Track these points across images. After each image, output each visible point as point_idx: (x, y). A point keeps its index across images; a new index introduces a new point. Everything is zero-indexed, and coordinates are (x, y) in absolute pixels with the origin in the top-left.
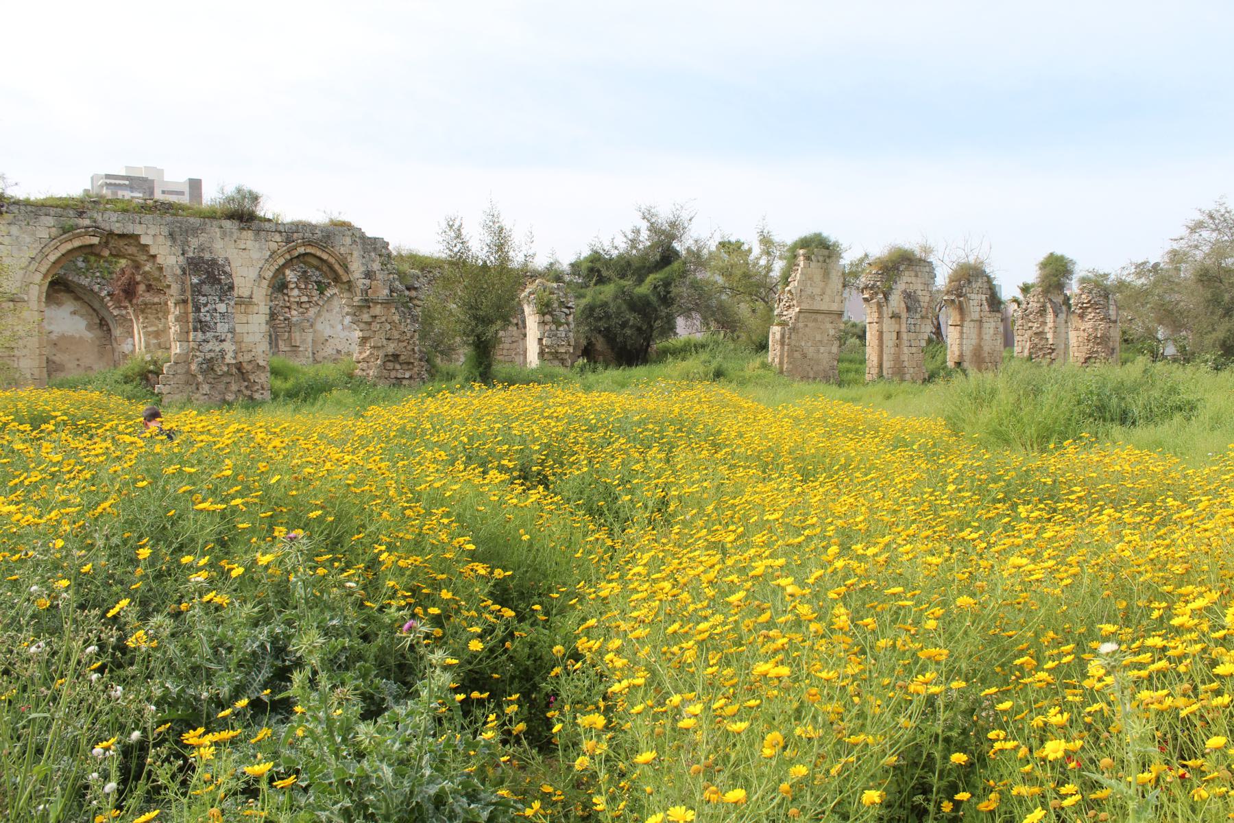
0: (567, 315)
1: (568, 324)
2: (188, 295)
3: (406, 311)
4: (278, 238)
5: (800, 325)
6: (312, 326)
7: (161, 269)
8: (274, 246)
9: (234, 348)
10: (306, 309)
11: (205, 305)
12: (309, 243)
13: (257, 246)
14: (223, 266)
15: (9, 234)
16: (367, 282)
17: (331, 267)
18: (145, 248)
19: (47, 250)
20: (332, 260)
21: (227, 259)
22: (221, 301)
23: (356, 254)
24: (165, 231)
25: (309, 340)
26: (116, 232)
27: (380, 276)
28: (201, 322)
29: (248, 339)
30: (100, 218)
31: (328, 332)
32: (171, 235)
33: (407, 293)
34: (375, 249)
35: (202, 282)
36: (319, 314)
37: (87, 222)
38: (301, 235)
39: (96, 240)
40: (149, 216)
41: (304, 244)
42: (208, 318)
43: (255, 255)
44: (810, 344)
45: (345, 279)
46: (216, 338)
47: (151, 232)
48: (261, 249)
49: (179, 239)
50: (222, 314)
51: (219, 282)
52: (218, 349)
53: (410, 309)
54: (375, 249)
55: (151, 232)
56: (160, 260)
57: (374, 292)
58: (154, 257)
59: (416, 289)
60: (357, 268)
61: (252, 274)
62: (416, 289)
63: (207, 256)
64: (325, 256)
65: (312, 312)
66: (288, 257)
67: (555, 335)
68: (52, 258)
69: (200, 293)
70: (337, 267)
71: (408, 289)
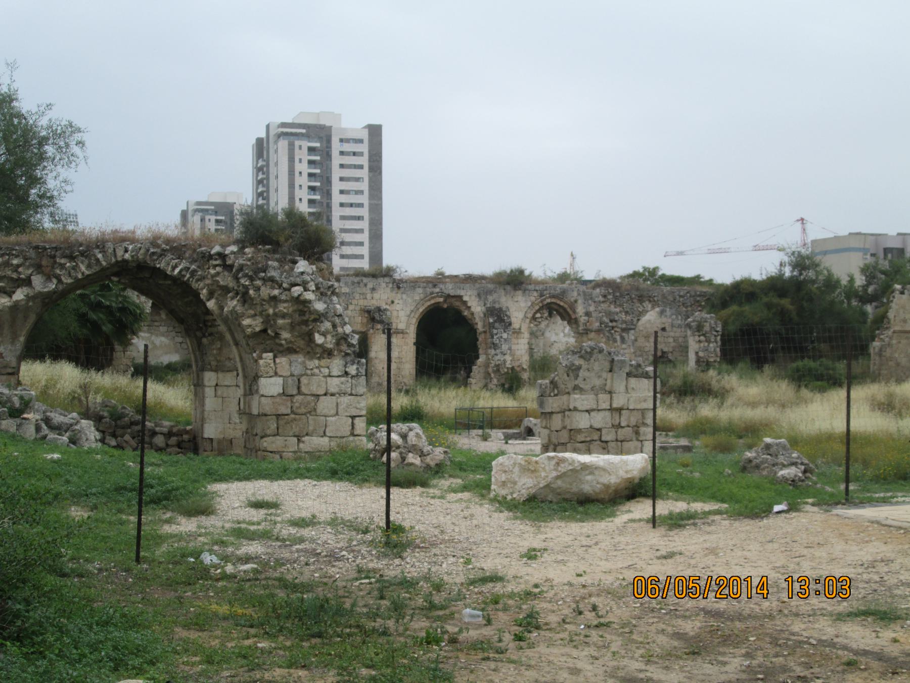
0: (715, 336)
1: (716, 342)
2: (487, 328)
3: (610, 336)
4: (535, 294)
5: (894, 342)
6: (543, 334)
7: (473, 314)
8: (533, 299)
9: (510, 358)
10: (540, 322)
11: (496, 334)
12: (553, 297)
13: (524, 299)
14: (506, 311)
15: (402, 298)
16: (586, 318)
17: (565, 309)
18: (465, 303)
19: (418, 306)
20: (566, 306)
21: (507, 307)
22: (505, 332)
23: (580, 302)
24: (475, 293)
25: (541, 344)
26: (452, 294)
27: (594, 315)
28: (493, 344)
29: (518, 353)
30: (443, 288)
31: (553, 338)
32: (479, 295)
33: (610, 324)
34: (591, 298)
35: (495, 321)
36: (547, 326)
37: (437, 290)
38: (548, 292)
39: (441, 300)
40: (468, 285)
41: (550, 297)
42: (498, 342)
43: (523, 304)
44: (902, 356)
45: (573, 317)
46: (502, 353)
47: (469, 293)
48: (526, 301)
49: (483, 297)
50: (505, 340)
51: (503, 321)
52: (502, 359)
53: (612, 334)
54: (591, 298)
55: (469, 293)
56: (473, 309)
57: (590, 325)
58: (470, 307)
59: (616, 321)
60: (580, 309)
61: (521, 315)
62: (616, 321)
63: (497, 306)
64: (562, 304)
65: (543, 325)
66: (541, 305)
67: (707, 350)
68: (421, 310)
69: (494, 327)
70: (569, 310)
71: (611, 321)
